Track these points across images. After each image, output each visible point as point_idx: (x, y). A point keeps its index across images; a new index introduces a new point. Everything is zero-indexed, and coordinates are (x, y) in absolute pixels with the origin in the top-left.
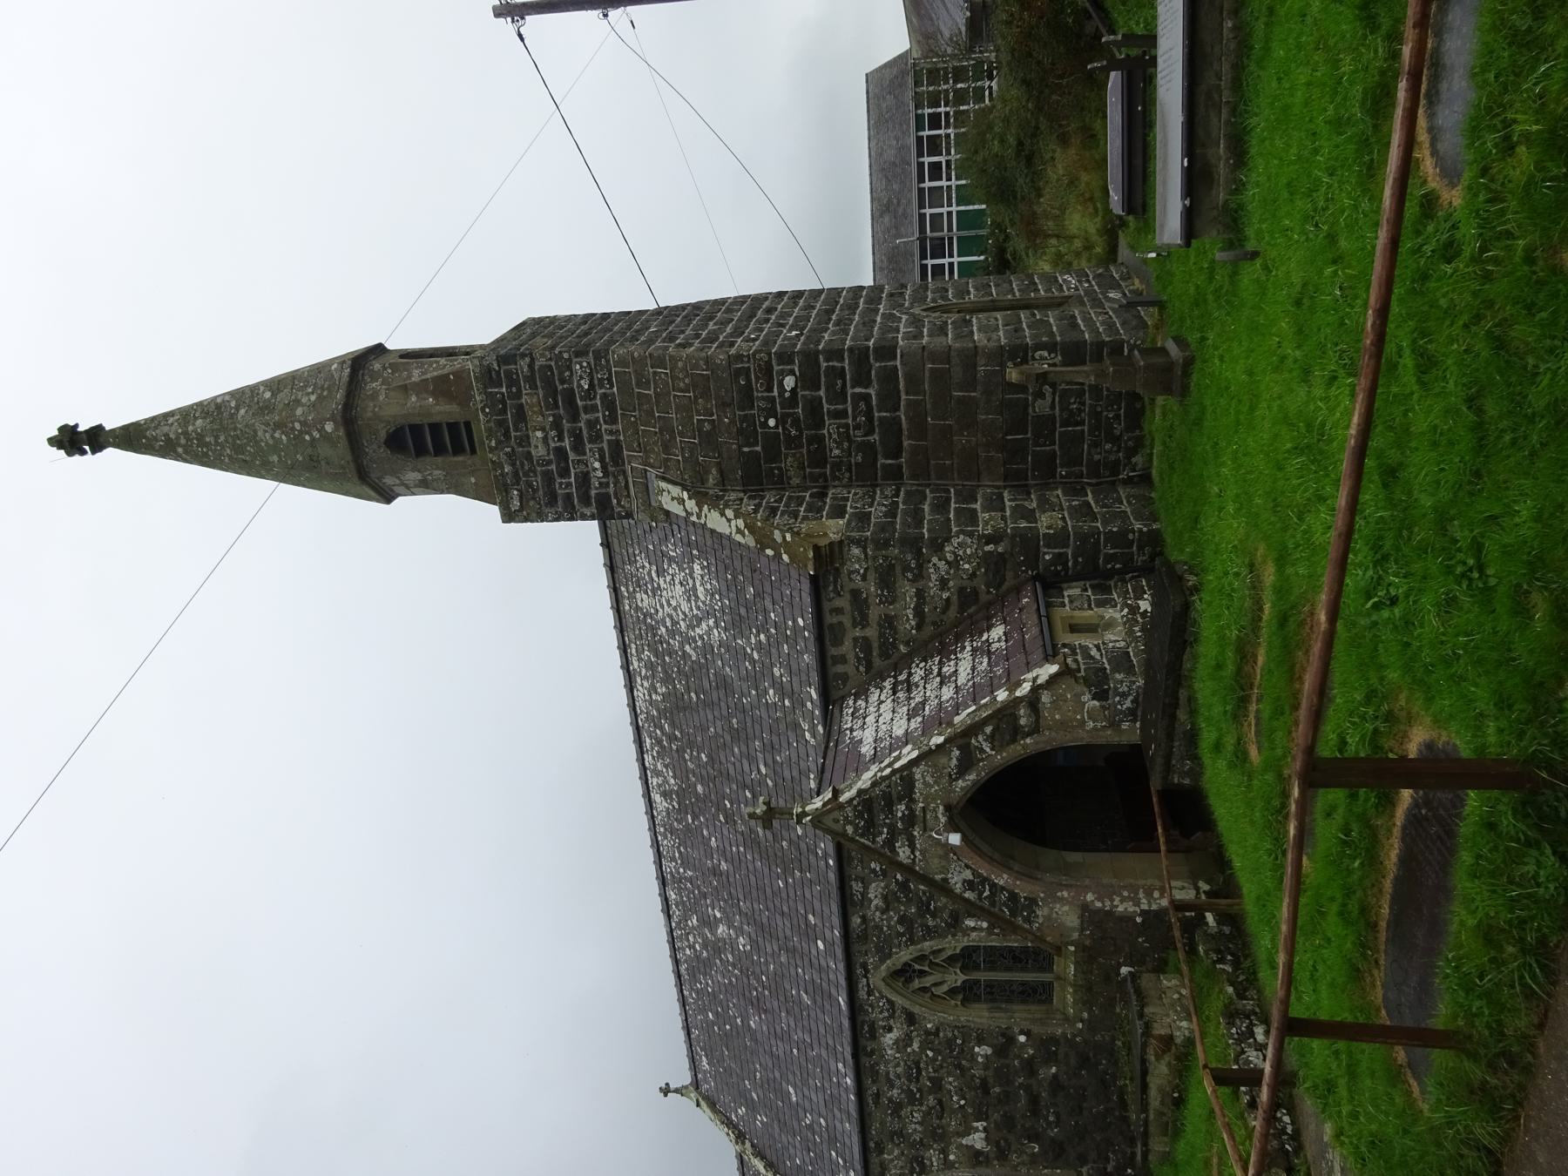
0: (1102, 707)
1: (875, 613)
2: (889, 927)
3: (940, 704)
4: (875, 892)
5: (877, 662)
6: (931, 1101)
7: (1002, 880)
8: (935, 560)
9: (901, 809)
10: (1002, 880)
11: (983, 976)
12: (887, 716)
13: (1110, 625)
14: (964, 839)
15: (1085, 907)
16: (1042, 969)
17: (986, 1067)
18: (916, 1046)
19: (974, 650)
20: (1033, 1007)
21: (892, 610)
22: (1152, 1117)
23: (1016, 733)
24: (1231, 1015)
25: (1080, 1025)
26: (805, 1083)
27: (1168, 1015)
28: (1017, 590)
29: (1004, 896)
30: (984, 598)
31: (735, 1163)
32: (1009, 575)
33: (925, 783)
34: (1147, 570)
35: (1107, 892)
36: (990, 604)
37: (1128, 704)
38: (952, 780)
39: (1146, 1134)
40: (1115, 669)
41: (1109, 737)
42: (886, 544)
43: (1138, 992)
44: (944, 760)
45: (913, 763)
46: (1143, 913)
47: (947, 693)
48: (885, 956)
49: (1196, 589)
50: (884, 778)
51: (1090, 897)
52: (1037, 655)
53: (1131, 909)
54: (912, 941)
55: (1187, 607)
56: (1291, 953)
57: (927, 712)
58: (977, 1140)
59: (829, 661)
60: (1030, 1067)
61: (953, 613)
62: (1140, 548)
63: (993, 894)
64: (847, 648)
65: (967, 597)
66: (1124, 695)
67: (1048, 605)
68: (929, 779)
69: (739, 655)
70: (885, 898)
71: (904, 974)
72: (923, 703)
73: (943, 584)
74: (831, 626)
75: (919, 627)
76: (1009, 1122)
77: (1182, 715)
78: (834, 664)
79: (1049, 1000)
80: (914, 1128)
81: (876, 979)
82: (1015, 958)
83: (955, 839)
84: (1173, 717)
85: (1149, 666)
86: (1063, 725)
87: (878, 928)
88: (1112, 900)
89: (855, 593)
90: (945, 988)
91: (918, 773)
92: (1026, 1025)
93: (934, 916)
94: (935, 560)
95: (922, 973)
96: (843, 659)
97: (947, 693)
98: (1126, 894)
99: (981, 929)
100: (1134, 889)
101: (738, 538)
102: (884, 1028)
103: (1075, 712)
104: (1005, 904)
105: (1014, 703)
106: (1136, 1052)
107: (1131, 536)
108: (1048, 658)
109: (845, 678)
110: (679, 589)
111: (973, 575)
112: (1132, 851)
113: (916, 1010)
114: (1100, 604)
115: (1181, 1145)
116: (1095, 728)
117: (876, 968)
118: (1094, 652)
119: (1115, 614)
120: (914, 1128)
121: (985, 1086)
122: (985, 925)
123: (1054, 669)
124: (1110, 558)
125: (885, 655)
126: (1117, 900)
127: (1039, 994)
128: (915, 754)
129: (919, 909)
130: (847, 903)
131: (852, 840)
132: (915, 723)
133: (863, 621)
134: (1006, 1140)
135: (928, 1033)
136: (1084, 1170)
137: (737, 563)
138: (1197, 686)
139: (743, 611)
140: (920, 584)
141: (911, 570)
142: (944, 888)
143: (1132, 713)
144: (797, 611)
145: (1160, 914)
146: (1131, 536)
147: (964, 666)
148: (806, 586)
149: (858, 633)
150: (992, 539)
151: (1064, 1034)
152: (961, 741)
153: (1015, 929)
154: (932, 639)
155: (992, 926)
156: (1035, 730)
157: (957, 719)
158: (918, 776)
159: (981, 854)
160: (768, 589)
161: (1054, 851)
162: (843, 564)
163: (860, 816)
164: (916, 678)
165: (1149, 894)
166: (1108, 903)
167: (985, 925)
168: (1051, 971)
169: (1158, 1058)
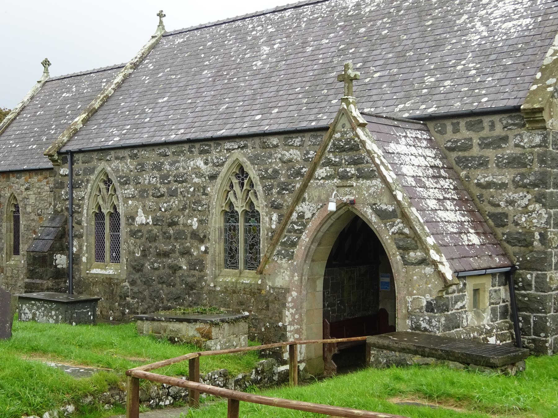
0: (422, 307)
1: (490, 153)
2: (271, 163)
3: (424, 198)
4: (295, 154)
5: (454, 155)
6: (163, 190)
7: (305, 238)
8: (529, 196)
9: (352, 170)
10: (305, 238)
11: (241, 225)
12: (416, 161)
13: (478, 316)
14: (332, 213)
15: (287, 290)
16: (246, 262)
17: (185, 225)
18: (196, 180)
19: (462, 223)
20: (222, 255)
21: (492, 165)
22: (163, 324)
23: (404, 249)
24: (225, 375)
25: (212, 285)
26: (170, 108)
27: (223, 338)
28: (505, 255)
29: (294, 238)
30: (499, 231)
31: (119, 63)
32: (516, 249)
33: (370, 187)
34: (517, 343)
35: (298, 307)
36: (495, 235)
37: (424, 325)
38: (372, 205)
39: (153, 320)
40: (447, 318)
41: (401, 311)
42: (542, 161)
43: (237, 320)
44: (385, 199)
45: (384, 179)
46: (285, 327)
47: (432, 204)
48: (253, 160)
49: (506, 374)
50: (373, 159)
51: (294, 294)
52: (459, 266)
53: (287, 320)
54: (262, 178)
55: (493, 367)
56: (278, 405)
57: (419, 189)
58: (141, 218)
59: (455, 121)
60: (186, 253)
61: (489, 209)
62: (534, 341)
63: (295, 231)
64: (465, 133)
65: (500, 219)
66: (429, 322)
67: (494, 275)
68: (372, 190)
69: (460, 56)
70: (290, 161)
71: (241, 173)
72: (424, 187)
73: (511, 203)
74: (481, 122)
75: (479, 185)
76: (153, 239)
77: (417, 359)
78: (453, 124)
79: (227, 266)
80: (147, 179)
81: (238, 155)
83: (332, 207)
84: (416, 353)
85: (451, 340)
86: (409, 281)
88: (292, 308)
89: (505, 139)
90: (233, 200)
91: (377, 182)
92: (211, 251)
93: (279, 193)
94: (529, 196)
95: (242, 185)
96: (456, 130)
97: (432, 204)
98: (297, 317)
99: (271, 224)
100: (300, 322)
101: (550, 51)
102: (207, 160)
103: (418, 290)
104: (289, 238)
105: (426, 250)
106: (201, 317)
107: (543, 334)
108: (456, 272)
109: (442, 132)
110: (510, 8)
111: (517, 224)
112: (324, 322)
113: (219, 180)
114: (493, 311)
115: (147, 340)
116: (406, 302)
118: (460, 304)
119: (486, 320)
120: (147, 179)
121: (173, 224)
122: (274, 227)
123: (449, 275)
124: (526, 320)
125: (459, 161)
126: (293, 311)
127: (231, 259)
128: (390, 180)
131: (331, 137)
132: (411, 181)
133: (485, 144)
134: (142, 236)
135: (204, 188)
136: (127, 284)
137: (530, 51)
138: (438, 370)
139: (493, 57)
140: (511, 186)
141: (522, 180)
142: (299, 199)
143: (418, 327)
144: (492, 97)
145: (283, 337)
146: (543, 334)
147: (451, 216)
148: (512, 103)
149: (476, 141)
150: (543, 237)
151: (206, 275)
152: (398, 212)
153: (274, 245)
154: (470, 193)
155: (273, 231)
156: (406, 263)
157: (414, 210)
158: (374, 182)
159: (322, 224)
160: (510, 75)
161: (323, 272)
162: (528, 130)
163: (347, 142)
164: (442, 182)
165: (297, 331)
166: (291, 305)
167: (274, 227)
168: (245, 268)
169: (198, 330)
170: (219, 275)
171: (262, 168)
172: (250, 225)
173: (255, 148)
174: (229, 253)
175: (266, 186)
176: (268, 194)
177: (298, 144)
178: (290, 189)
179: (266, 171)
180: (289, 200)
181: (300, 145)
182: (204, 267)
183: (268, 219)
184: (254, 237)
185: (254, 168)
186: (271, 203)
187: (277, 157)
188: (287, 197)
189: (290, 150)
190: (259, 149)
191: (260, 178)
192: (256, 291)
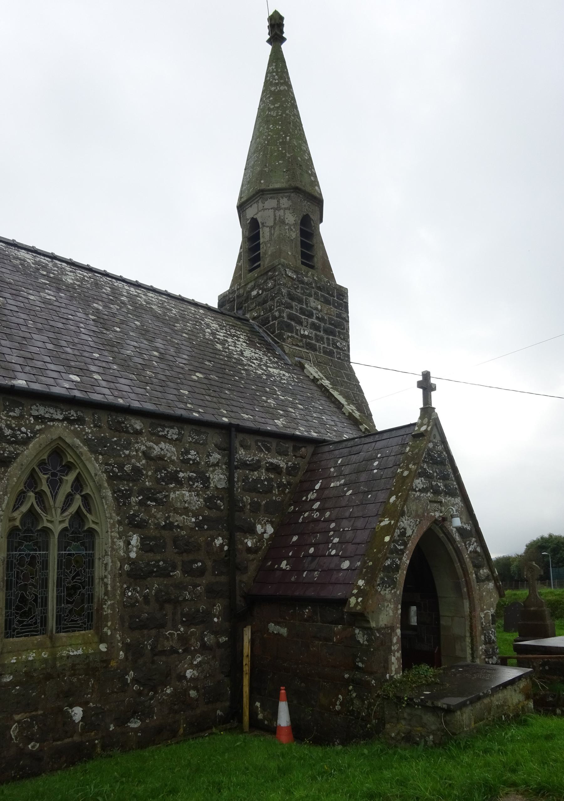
2: (129, 455)
16: (59, 620)
48: (95, 446)
54: (112, 478)
70: (161, 458)
82: (75, 588)
87: (128, 446)
93: (140, 503)
99: (128, 551)
117: (77, 434)
122: (133, 555)
129: (149, 489)
130: (157, 419)
155: (133, 562)
167: (133, 555)
171: (111, 461)
173: (100, 427)
174: (18, 608)
175: (120, 491)
176: (124, 504)
177: (175, 437)
178: (161, 499)
179: (121, 467)
180: (158, 516)
181: (177, 439)
183: (122, 544)
184: (78, 574)
185: (97, 460)
186: (127, 518)
187: (139, 449)
188: (154, 510)
189: (160, 443)
191: (109, 477)
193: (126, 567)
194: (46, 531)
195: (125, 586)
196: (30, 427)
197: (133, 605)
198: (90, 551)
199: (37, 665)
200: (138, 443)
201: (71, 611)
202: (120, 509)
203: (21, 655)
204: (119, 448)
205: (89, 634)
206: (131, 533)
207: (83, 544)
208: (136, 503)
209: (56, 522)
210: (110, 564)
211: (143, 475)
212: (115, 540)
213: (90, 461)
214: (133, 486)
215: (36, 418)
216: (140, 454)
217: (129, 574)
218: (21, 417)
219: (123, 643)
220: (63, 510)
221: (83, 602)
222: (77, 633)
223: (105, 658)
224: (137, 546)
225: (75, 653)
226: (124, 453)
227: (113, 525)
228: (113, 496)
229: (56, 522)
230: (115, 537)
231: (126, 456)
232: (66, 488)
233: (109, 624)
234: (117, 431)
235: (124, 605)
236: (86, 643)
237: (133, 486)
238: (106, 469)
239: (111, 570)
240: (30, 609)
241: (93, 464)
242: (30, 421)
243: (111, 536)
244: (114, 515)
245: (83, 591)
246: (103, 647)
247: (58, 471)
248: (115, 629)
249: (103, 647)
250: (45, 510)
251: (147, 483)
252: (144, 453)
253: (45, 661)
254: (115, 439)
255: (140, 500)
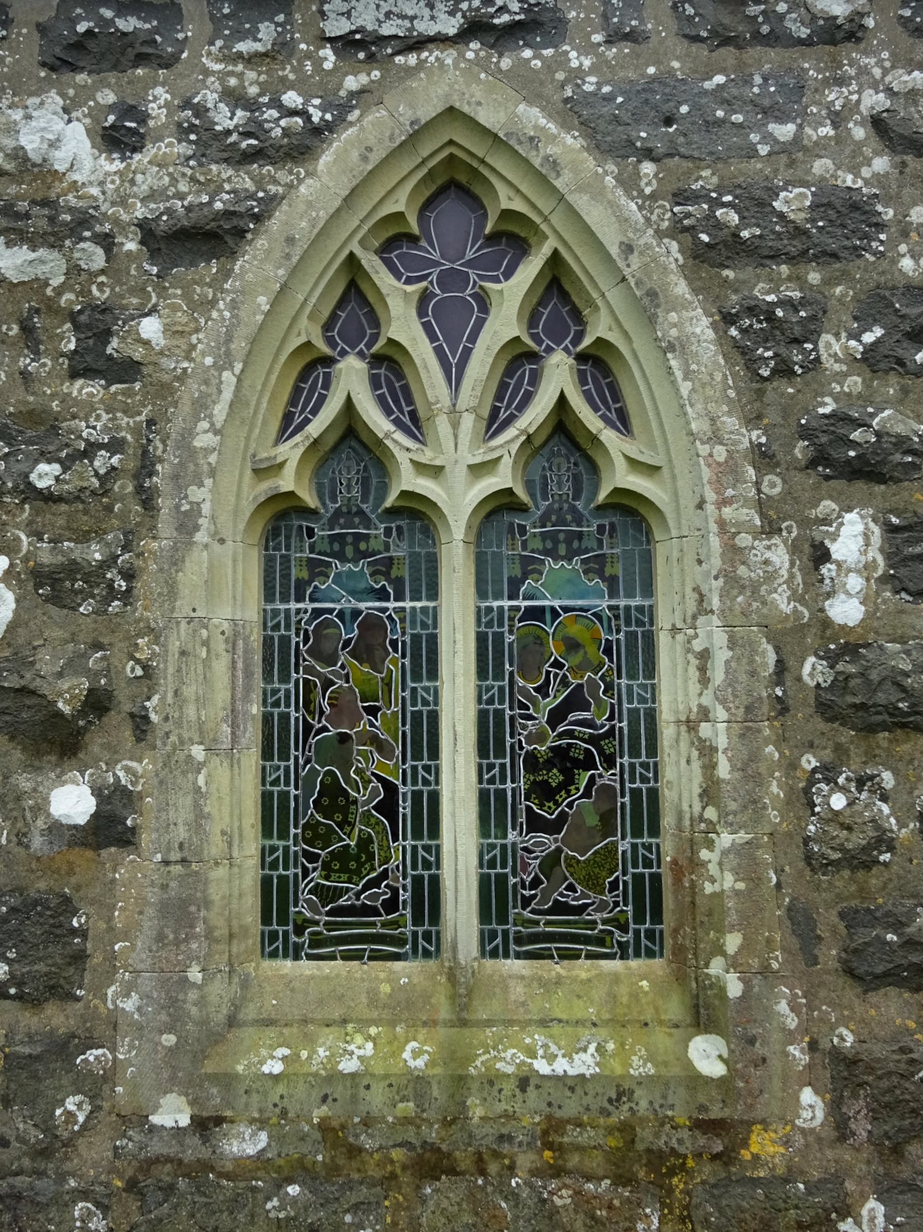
2: (794, 153)
16: (494, 898)
20: (251, 847)
25: (173, 1113)
54: (711, 253)
79: (282, 925)
87: (790, 100)
92: (159, 827)
93: (872, 361)
117: (528, 86)
127: (340, 871)
151: (110, 1028)
155: (845, 647)
167: (846, 611)
170: (232, 1022)
171: (706, 179)
172: (535, 613)
173: (632, 37)
179: (757, 203)
182: (79, 958)
183: (780, 557)
184: (576, 701)
185: (630, 183)
186: (805, 433)
187: (851, 108)
190: (682, 47)
192: (686, 1142)
193: (813, 671)
194: (417, 514)
195: (809, 762)
196: (323, 87)
197: (861, 861)
198: (630, 595)
199: (376, 1098)
200: (841, 82)
201: (551, 862)
202: (760, 393)
203: (310, 1041)
204: (738, 118)
205: (641, 974)
206: (828, 506)
207: (597, 566)
208: (850, 359)
209: (457, 468)
210: (722, 655)
211: (880, 226)
212: (744, 540)
213: (597, 191)
214: (829, 282)
215: (346, 45)
216: (859, 133)
217: (826, 706)
218: (282, 50)
219: (813, 1046)
220: (495, 423)
221: (607, 825)
222: (583, 968)
223: (716, 1112)
224: (869, 567)
225: (561, 1066)
226: (768, 138)
227: (728, 471)
228: (722, 337)
229: (457, 468)
230: (741, 527)
231: (781, 149)
232: (504, 323)
233: (733, 942)
234: (726, 41)
235: (809, 858)
236: (621, 1021)
237: (829, 282)
238: (676, 220)
239: (731, 680)
240: (365, 843)
241: (613, 205)
242: (318, 62)
243: (722, 524)
244: (731, 422)
245: (607, 777)
246: (707, 1055)
247: (470, 264)
248: (765, 971)
249: (707, 1055)
250: (414, 425)
251: (907, 263)
252: (878, 123)
253: (417, 1084)
254: (720, 79)
255: (870, 349)
